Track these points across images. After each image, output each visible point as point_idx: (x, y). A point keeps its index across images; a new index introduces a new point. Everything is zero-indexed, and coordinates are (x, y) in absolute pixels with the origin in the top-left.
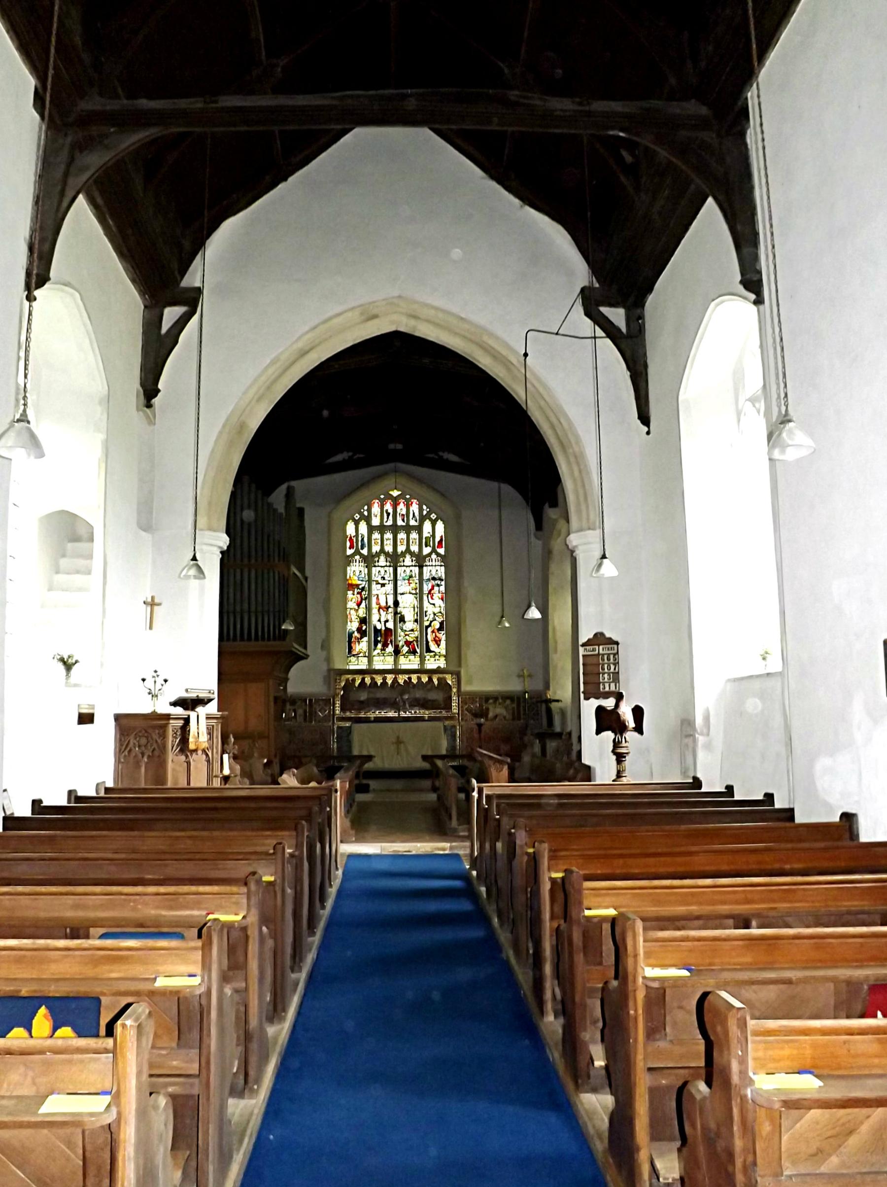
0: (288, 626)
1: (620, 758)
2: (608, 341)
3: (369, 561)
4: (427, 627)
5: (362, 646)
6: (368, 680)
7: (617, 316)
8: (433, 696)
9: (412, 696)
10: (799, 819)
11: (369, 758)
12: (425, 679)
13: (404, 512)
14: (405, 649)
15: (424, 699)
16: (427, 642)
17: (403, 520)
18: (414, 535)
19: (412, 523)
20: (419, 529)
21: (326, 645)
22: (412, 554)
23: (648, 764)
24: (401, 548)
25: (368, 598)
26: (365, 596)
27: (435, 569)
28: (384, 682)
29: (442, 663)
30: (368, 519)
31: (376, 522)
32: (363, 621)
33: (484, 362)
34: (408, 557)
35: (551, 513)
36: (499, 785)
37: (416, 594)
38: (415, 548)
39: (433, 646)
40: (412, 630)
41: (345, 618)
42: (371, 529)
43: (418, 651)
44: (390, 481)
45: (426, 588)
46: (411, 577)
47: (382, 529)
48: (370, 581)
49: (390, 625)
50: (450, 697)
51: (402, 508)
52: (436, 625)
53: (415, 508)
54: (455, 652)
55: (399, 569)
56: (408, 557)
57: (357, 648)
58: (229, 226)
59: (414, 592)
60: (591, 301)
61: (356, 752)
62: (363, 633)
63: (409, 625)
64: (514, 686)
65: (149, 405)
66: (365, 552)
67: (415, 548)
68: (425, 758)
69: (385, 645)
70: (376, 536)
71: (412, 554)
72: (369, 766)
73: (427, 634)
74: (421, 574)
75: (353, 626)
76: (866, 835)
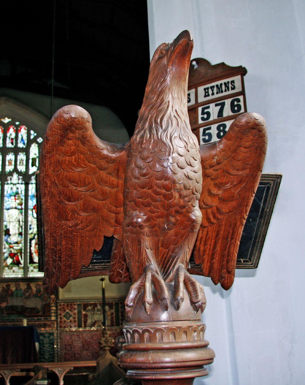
4: (31, 240)
9: (10, 304)
13: (13, 136)
14: (9, 261)
15: (22, 306)
16: (31, 254)
17: (12, 143)
19: (21, 145)
20: (26, 151)
22: (20, 173)
34: (15, 176)
37: (22, 209)
40: (17, 243)
43: (22, 262)
46: (17, 193)
50: (49, 304)
51: (11, 132)
53: (23, 132)
55: (6, 187)
56: (15, 176)
59: (20, 207)
63: (14, 238)
71: (20, 173)
73: (30, 246)
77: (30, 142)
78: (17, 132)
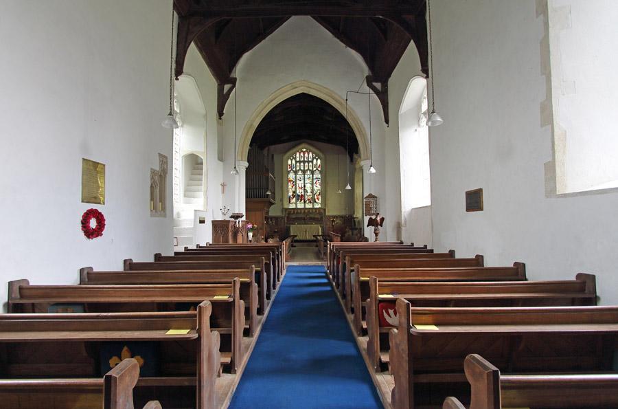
0: (268, 193)
1: (376, 235)
2: (375, 95)
3: (296, 173)
5: (294, 200)
6: (296, 211)
7: (378, 85)
8: (317, 216)
10: (435, 252)
11: (296, 236)
12: (314, 211)
18: (311, 164)
20: (312, 162)
21: (282, 200)
23: (387, 236)
24: (306, 168)
25: (296, 185)
26: (295, 184)
27: (317, 175)
28: (301, 213)
29: (319, 206)
30: (295, 159)
31: (298, 159)
32: (294, 192)
33: (333, 103)
35: (355, 156)
36: (337, 243)
38: (311, 168)
39: (317, 200)
41: (288, 191)
42: (296, 162)
44: (303, 145)
45: (314, 182)
47: (300, 162)
48: (296, 179)
49: (303, 194)
51: (306, 155)
52: (318, 193)
53: (311, 154)
54: (324, 202)
57: (292, 201)
58: (246, 56)
60: (370, 81)
61: (292, 234)
62: (294, 196)
63: (309, 194)
64: (343, 213)
65: (220, 119)
66: (294, 169)
67: (311, 168)
68: (314, 236)
69: (301, 200)
70: (298, 164)
72: (295, 238)
74: (313, 176)
75: (291, 194)
76: (457, 256)
77: (313, 159)
78: (308, 154)
